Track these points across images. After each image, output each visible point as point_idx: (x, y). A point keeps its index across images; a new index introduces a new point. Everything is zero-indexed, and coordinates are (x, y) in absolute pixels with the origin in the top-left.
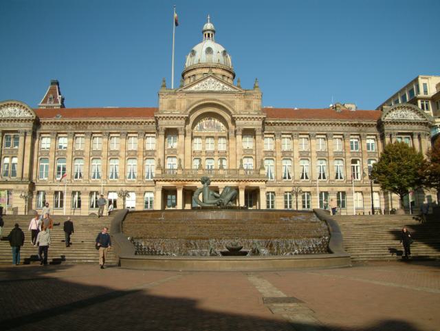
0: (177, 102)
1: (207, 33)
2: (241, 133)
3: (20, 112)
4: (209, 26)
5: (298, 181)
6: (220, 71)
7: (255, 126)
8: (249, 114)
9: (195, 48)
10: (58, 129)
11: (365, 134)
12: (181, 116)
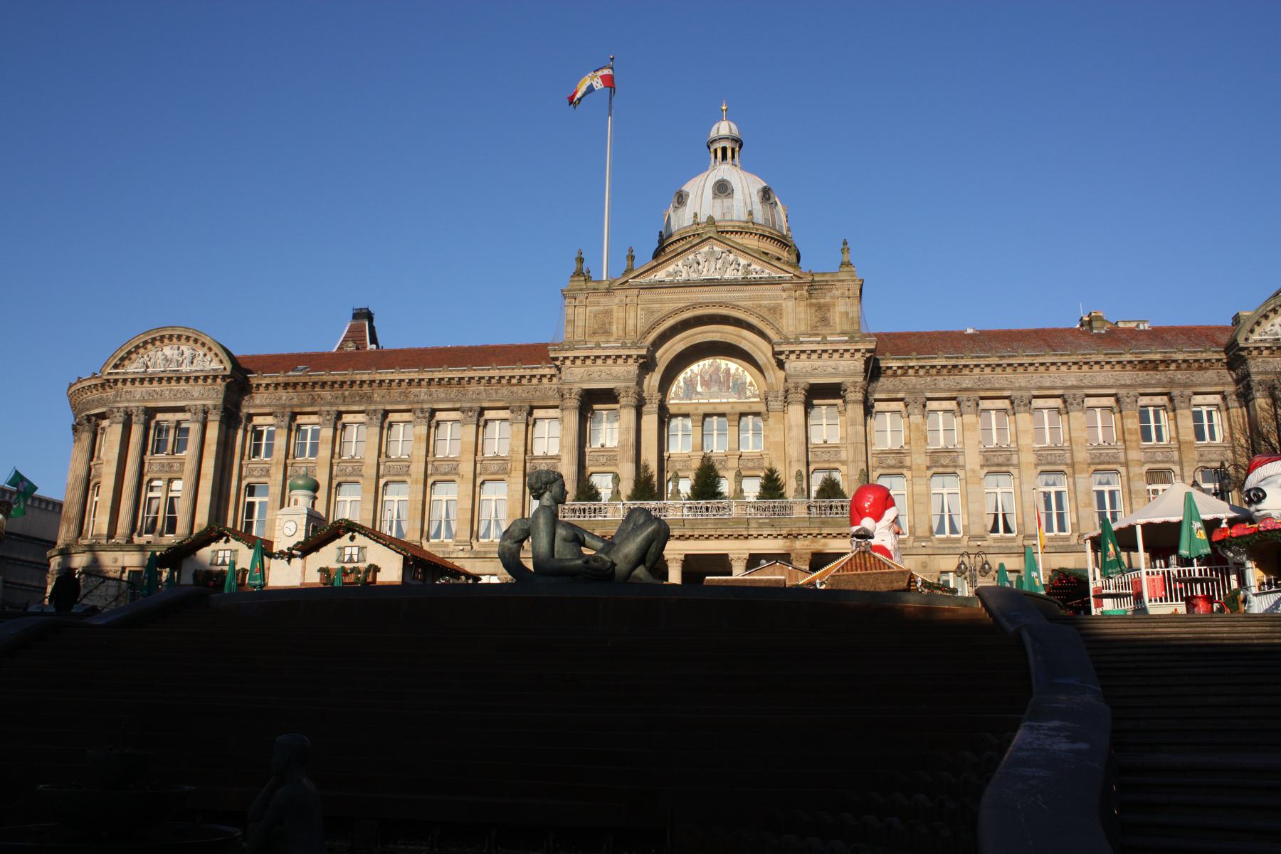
0: (615, 315)
1: (718, 146)
2: (801, 397)
3: (193, 357)
4: (724, 128)
5: (982, 538)
6: (752, 242)
7: (845, 375)
8: (824, 341)
9: (686, 188)
10: (295, 401)
11: (1188, 392)
12: (625, 352)
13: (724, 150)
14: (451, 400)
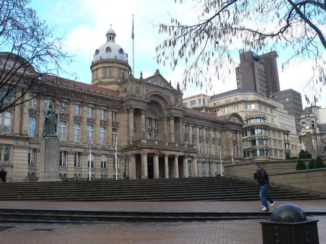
13: (110, 37)
14: (93, 102)
